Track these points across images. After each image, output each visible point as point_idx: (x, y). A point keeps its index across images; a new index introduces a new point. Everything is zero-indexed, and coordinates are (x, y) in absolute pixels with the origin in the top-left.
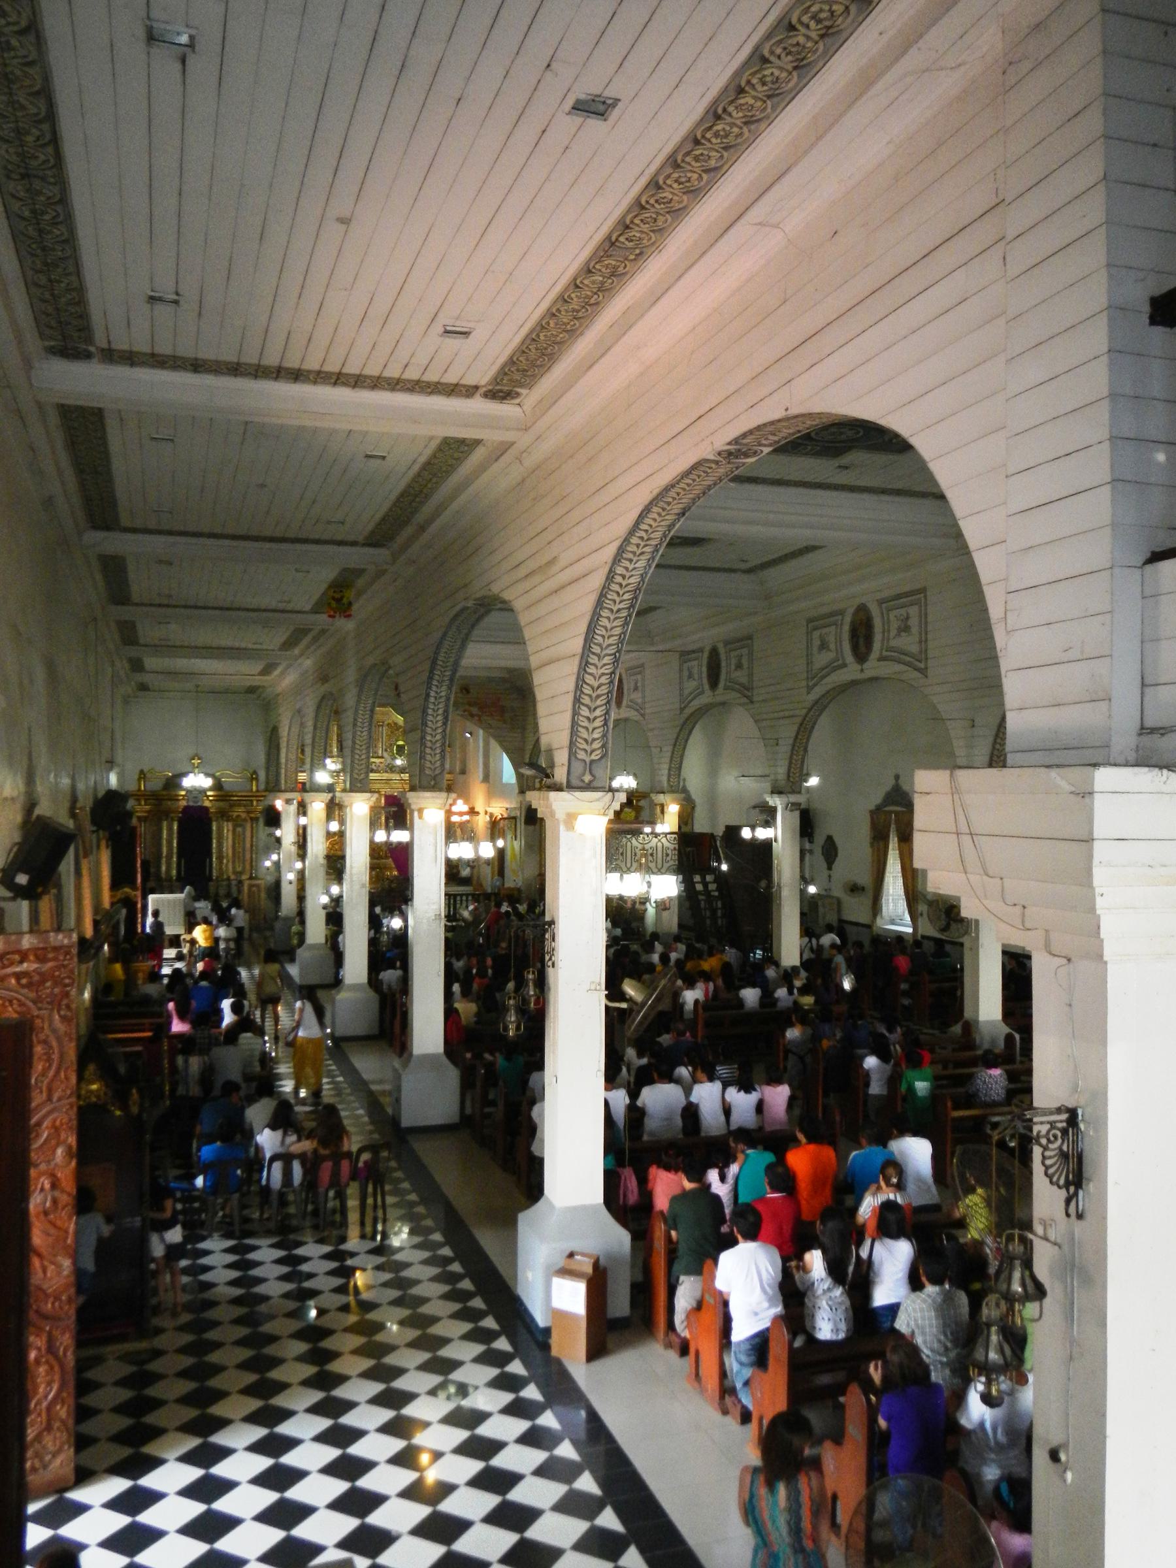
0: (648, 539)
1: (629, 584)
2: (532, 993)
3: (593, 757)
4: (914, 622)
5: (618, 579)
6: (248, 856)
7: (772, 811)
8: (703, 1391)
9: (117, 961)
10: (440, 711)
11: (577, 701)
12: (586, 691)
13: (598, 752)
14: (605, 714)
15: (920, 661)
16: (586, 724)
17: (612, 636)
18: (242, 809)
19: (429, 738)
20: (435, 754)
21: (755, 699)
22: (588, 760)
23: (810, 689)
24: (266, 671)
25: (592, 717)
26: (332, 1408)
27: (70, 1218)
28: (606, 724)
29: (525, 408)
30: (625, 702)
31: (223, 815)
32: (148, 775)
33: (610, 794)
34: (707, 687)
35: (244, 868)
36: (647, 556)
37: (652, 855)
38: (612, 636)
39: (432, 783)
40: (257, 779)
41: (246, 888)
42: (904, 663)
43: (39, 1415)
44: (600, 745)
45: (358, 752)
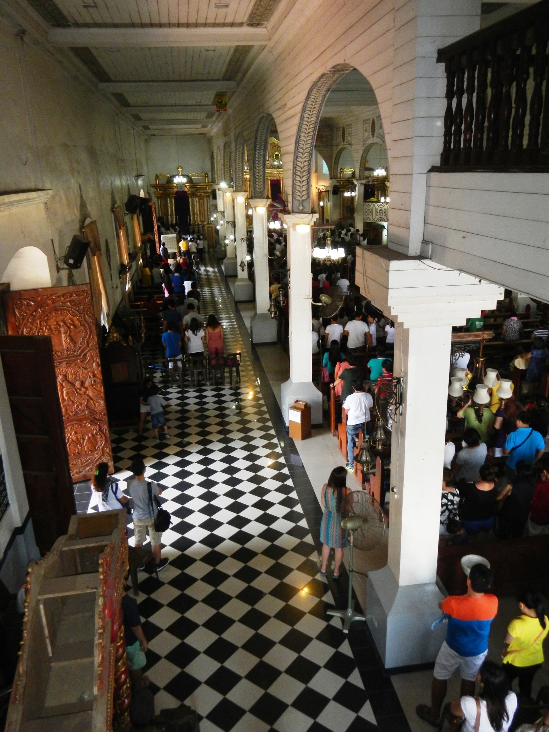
0: (316, 102)
2: (281, 299)
3: (303, 198)
5: (306, 119)
8: (342, 452)
9: (147, 267)
10: (261, 162)
11: (294, 173)
12: (298, 169)
14: (307, 179)
17: (307, 144)
18: (202, 191)
19: (257, 174)
22: (301, 200)
24: (204, 127)
25: (301, 181)
26: (205, 452)
27: (101, 387)
29: (268, 28)
30: (376, 135)
31: (194, 195)
32: (160, 177)
33: (312, 214)
35: (205, 219)
36: (317, 109)
37: (385, 212)
39: (260, 195)
40: (208, 177)
41: (206, 228)
43: (99, 451)
44: (306, 193)
45: (238, 173)
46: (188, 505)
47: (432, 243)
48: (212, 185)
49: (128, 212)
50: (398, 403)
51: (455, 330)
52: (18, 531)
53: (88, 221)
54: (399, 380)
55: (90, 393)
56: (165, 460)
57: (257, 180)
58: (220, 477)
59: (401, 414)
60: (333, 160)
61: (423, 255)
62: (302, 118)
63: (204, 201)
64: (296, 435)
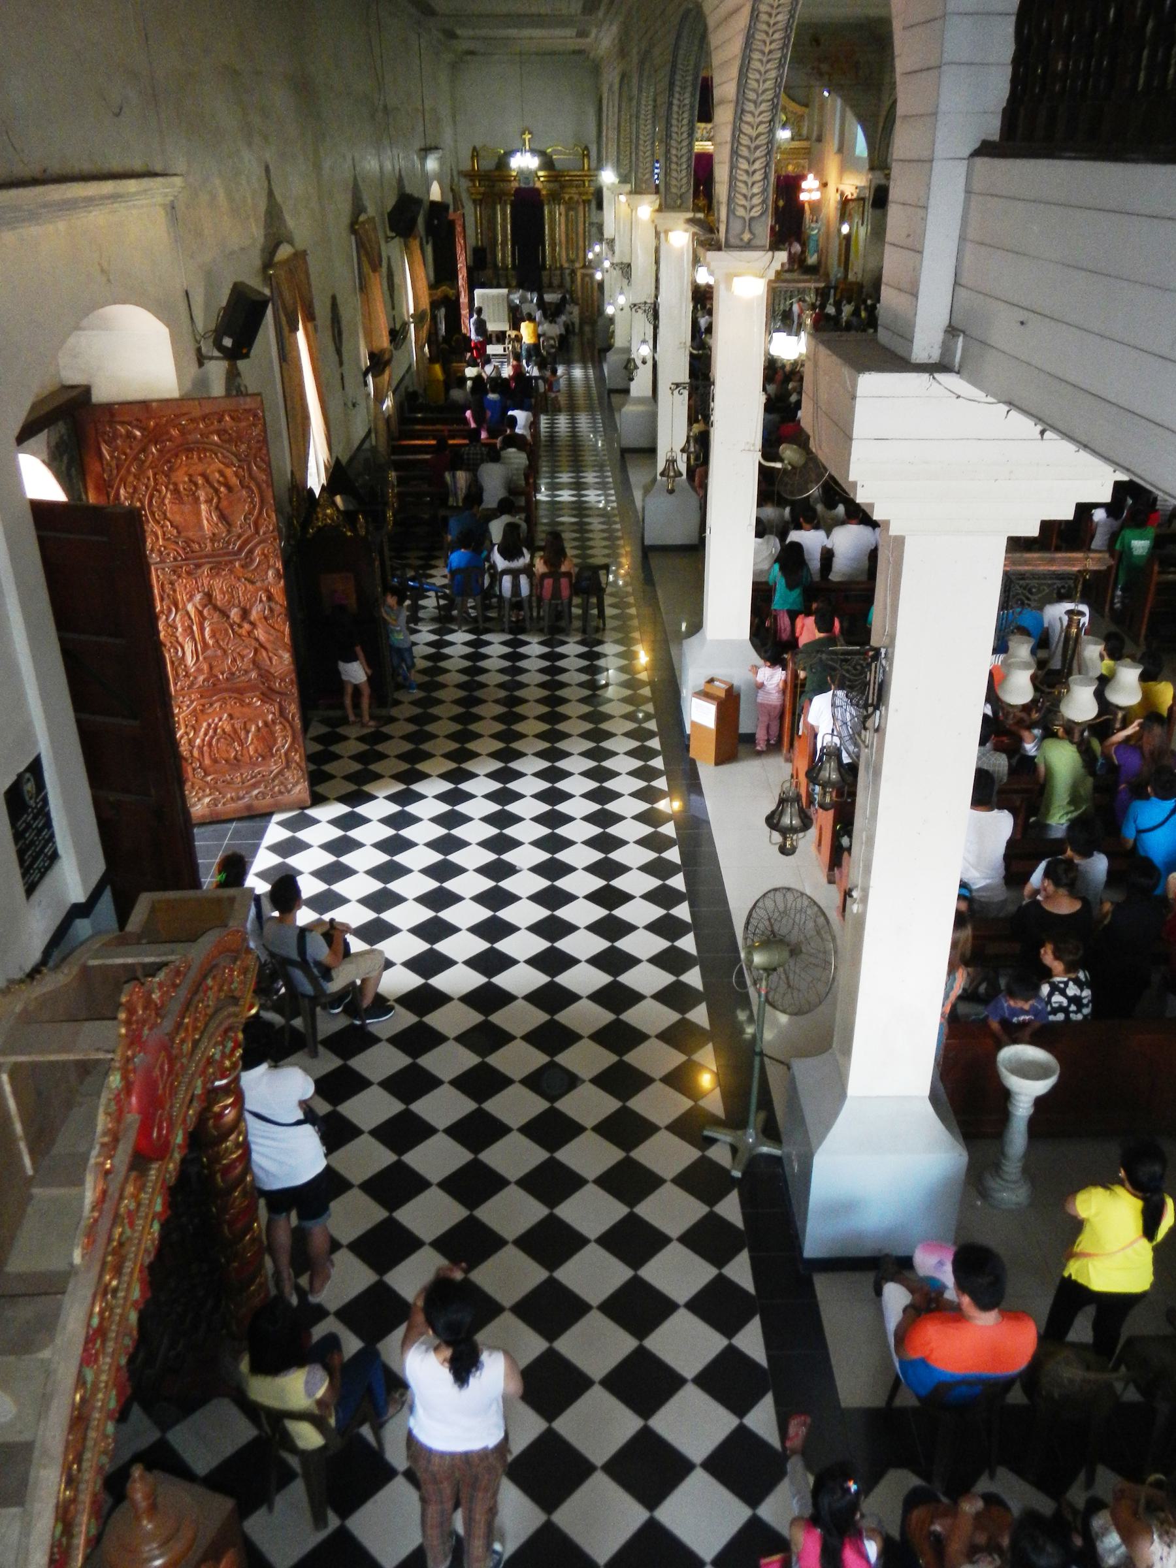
9: (437, 362)
10: (685, 122)
13: (759, 208)
18: (574, 190)
19: (674, 152)
24: (582, 34)
26: (505, 775)
27: (285, 624)
28: (766, 177)
31: (555, 197)
32: (482, 154)
33: (770, 253)
39: (679, 202)
40: (588, 156)
46: (452, 885)
47: (964, 332)
49: (394, 234)
50: (872, 705)
51: (1017, 545)
52: (79, 911)
53: (284, 252)
54: (877, 651)
55: (260, 633)
56: (418, 787)
58: (527, 831)
59: (877, 730)
60: (881, 124)
61: (946, 361)
63: (577, 214)
64: (703, 753)
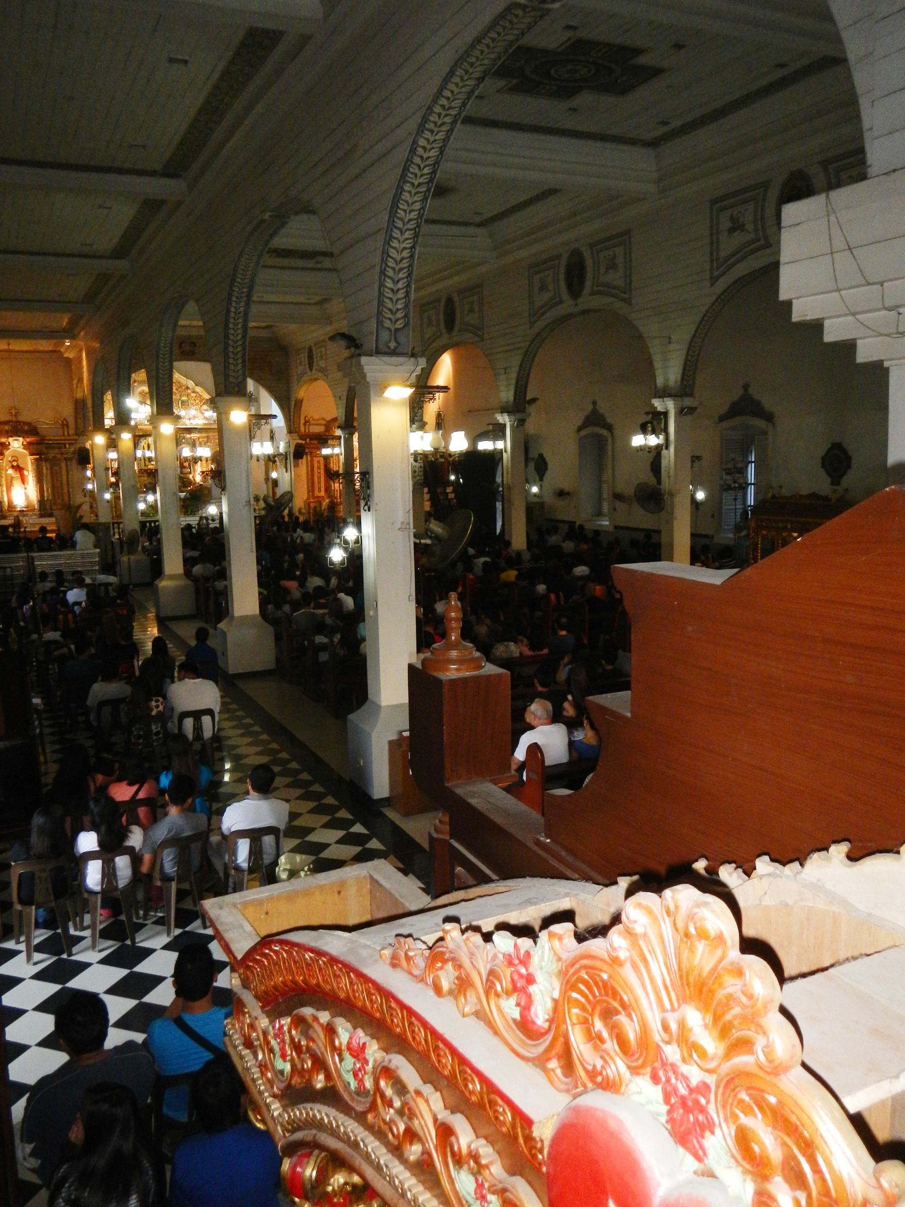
1: (429, 158)
4: (620, 260)
6: (66, 490)
7: (503, 427)
10: (240, 326)
12: (390, 264)
15: (625, 293)
16: (390, 295)
17: (413, 210)
18: (57, 451)
19: (231, 349)
20: (237, 364)
21: (486, 336)
22: (393, 329)
23: (532, 324)
33: (412, 359)
34: (444, 331)
38: (413, 210)
39: (237, 389)
40: (67, 426)
42: (612, 296)
48: (75, 440)
57: (231, 361)
62: (413, 151)
63: (61, 468)
